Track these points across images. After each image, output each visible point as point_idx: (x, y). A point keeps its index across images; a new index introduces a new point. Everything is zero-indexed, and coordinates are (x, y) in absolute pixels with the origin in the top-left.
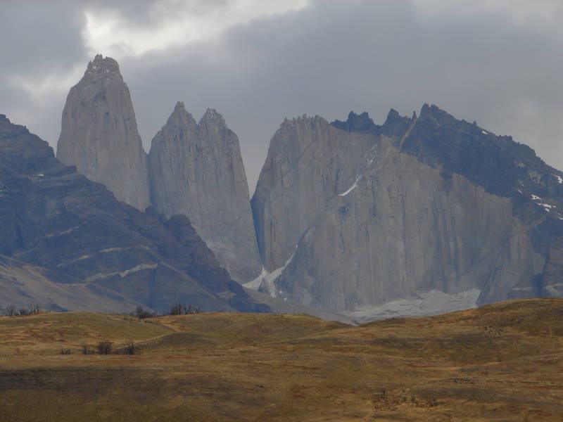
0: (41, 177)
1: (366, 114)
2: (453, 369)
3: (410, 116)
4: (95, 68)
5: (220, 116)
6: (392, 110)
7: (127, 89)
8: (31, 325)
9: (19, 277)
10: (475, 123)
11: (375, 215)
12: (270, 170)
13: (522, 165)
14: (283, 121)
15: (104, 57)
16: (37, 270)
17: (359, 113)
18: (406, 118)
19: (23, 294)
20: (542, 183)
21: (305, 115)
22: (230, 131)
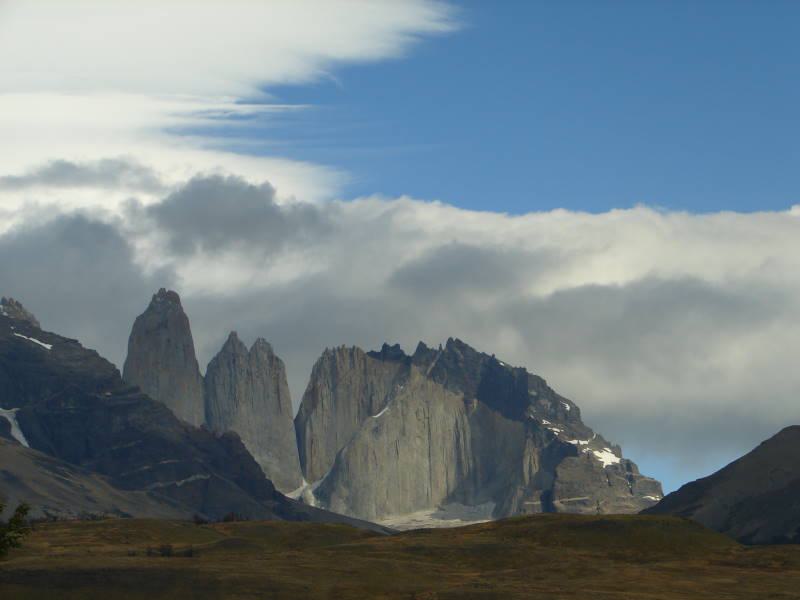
1: (397, 346)
2: (472, 575)
5: (268, 344)
6: (421, 343)
7: (186, 318)
8: (100, 529)
9: (87, 485)
10: (493, 356)
12: (312, 395)
13: (534, 393)
14: (323, 350)
16: (103, 479)
18: (432, 350)
19: (90, 499)
20: (553, 410)
21: (343, 346)
22: (277, 359)
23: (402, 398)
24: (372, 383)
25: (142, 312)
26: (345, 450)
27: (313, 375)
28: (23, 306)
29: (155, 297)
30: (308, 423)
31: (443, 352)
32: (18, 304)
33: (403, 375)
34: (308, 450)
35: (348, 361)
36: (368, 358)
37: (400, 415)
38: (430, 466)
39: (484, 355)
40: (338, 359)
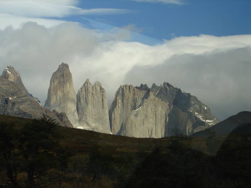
0: (15, 98)
1: (146, 85)
3: (160, 86)
4: (61, 67)
5: (100, 84)
6: (154, 84)
7: (71, 74)
10: (180, 89)
11: (146, 117)
13: (193, 103)
14: (120, 86)
15: (64, 63)
17: (144, 84)
18: (158, 86)
20: (199, 109)
21: (127, 84)
22: (103, 89)
23: (146, 103)
24: (136, 98)
25: (55, 71)
26: (125, 122)
27: (116, 95)
28: (15, 68)
29: (60, 66)
30: (113, 112)
31: (162, 87)
32: (12, 68)
33: (147, 96)
34: (113, 122)
35: (128, 90)
36: (135, 89)
37: (145, 110)
38: (156, 129)
39: (176, 88)
40: (125, 89)
